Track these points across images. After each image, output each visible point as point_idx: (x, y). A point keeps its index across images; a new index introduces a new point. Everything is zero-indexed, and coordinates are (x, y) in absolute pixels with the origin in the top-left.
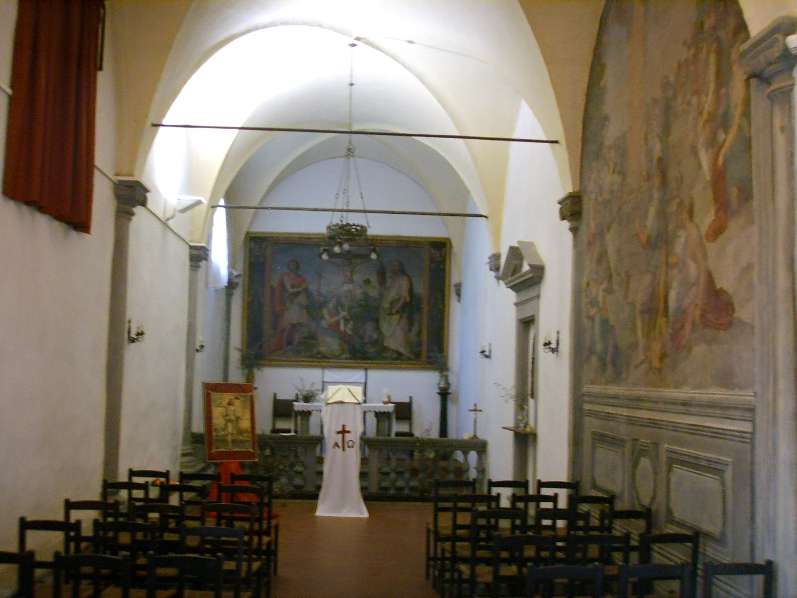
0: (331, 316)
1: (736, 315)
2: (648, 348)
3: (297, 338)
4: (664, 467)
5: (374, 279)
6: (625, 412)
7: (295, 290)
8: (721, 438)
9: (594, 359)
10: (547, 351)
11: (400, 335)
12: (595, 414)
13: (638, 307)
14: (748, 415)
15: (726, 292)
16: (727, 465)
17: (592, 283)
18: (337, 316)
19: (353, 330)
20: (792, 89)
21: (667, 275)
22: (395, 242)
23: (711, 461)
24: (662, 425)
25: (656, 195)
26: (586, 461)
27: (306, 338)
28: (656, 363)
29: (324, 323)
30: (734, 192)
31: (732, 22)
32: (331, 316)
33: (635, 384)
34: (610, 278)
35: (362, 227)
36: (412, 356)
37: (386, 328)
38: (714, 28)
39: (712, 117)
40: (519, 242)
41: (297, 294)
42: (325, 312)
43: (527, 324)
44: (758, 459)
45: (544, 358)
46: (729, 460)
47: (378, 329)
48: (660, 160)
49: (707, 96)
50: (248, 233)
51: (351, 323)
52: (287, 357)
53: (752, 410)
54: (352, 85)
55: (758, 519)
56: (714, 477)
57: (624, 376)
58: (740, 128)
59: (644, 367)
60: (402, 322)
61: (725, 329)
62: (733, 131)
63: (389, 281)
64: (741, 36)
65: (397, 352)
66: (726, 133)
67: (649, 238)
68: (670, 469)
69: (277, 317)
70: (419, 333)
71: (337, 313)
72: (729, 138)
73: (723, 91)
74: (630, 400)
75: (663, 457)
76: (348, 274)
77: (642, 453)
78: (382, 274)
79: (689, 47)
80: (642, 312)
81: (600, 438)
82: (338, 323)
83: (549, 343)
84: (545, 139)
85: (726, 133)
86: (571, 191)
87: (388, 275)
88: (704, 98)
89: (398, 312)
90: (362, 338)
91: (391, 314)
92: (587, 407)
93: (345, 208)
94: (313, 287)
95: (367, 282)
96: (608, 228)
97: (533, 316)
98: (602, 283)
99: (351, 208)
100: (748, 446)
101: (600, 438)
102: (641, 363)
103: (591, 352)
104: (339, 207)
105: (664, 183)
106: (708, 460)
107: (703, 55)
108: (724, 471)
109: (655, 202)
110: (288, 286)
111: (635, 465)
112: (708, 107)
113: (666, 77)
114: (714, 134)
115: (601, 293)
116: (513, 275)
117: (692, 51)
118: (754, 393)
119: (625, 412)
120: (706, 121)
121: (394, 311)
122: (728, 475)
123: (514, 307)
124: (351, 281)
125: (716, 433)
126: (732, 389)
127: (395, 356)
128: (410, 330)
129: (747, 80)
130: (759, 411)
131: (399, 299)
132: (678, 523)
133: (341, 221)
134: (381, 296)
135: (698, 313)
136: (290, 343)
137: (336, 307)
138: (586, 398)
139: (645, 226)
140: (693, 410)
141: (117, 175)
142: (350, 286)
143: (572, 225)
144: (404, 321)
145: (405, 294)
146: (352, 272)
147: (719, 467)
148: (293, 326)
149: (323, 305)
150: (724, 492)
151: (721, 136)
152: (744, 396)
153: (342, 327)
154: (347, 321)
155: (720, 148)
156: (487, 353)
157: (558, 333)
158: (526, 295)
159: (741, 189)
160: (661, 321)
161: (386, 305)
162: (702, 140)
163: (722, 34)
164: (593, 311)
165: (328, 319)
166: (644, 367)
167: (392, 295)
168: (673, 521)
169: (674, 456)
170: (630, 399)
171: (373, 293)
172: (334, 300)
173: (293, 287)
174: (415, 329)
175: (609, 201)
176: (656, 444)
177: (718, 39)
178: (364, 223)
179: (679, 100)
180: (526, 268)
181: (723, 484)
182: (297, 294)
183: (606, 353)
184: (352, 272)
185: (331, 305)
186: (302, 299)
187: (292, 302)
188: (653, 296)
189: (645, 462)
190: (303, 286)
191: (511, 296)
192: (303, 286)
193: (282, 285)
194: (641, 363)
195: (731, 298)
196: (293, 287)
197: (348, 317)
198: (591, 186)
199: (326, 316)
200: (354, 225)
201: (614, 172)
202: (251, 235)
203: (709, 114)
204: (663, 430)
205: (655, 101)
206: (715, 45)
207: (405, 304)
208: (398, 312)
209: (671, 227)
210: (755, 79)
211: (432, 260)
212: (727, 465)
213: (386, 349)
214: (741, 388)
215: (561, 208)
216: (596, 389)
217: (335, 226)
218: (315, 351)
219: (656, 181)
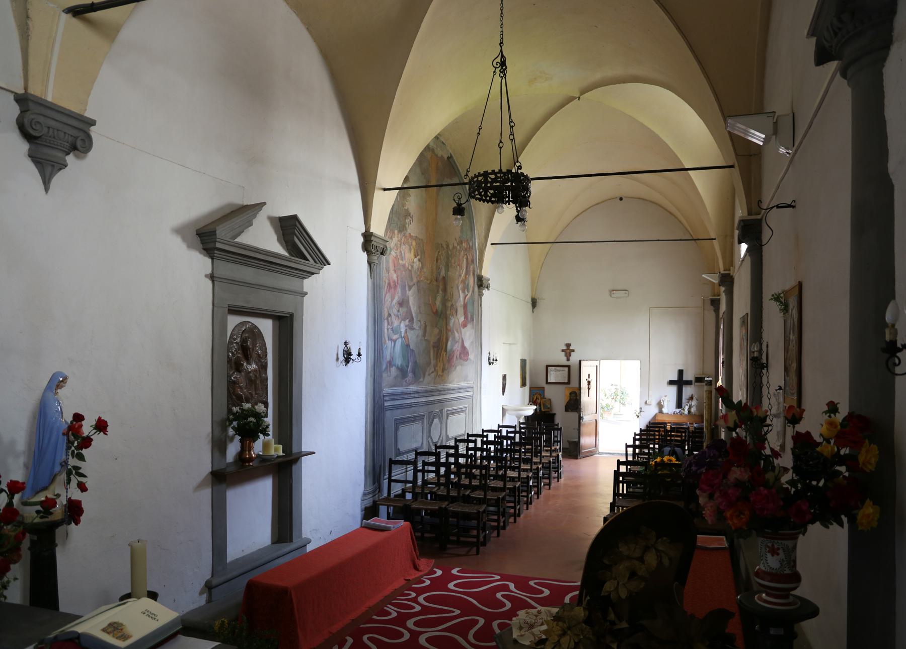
2: (436, 366)
6: (424, 399)
13: (432, 343)
28: (440, 373)
57: (421, 380)
59: (433, 375)
102: (432, 372)
119: (424, 399)
140: (456, 391)
152: (470, 384)
160: (443, 353)
169: (449, 412)
176: (441, 411)
188: (439, 340)
189: (436, 421)
194: (432, 372)
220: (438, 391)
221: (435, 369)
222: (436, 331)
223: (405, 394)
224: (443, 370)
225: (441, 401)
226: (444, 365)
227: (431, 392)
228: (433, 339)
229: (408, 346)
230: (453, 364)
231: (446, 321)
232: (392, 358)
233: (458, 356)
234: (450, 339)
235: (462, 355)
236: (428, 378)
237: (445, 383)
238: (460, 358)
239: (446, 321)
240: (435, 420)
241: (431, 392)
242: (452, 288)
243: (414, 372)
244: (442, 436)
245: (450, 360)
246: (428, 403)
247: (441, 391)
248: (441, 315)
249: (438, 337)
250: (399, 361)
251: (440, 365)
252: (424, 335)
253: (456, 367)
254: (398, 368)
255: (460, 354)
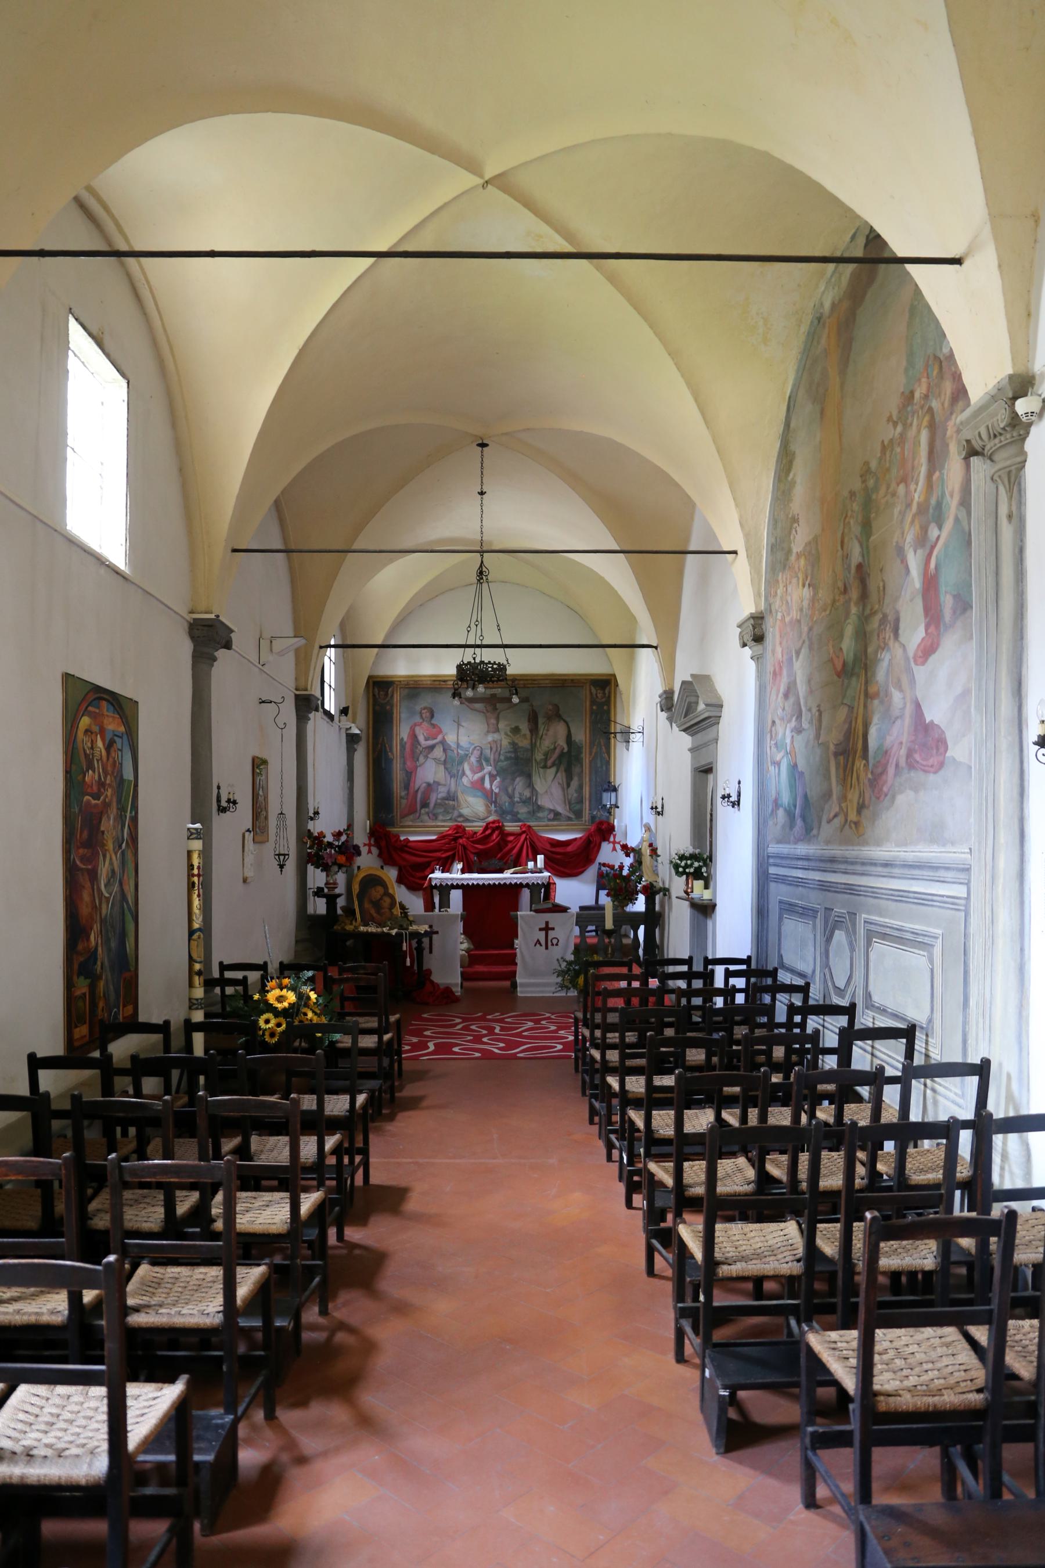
0: (475, 773)
1: (948, 754)
2: (843, 798)
3: (433, 799)
4: (862, 942)
5: (525, 728)
6: (817, 876)
7: (430, 743)
8: (932, 906)
9: (781, 812)
10: (726, 804)
11: (557, 792)
12: (782, 880)
13: (832, 747)
14: (962, 876)
15: (938, 726)
16: (937, 938)
17: (777, 721)
18: (480, 771)
19: (498, 787)
20: (1024, 466)
21: (865, 706)
22: (547, 682)
23: (917, 934)
24: (861, 891)
25: (854, 610)
26: (772, 937)
27: (444, 799)
28: (853, 816)
29: (465, 780)
30: (947, 602)
31: (948, 387)
32: (475, 773)
33: (828, 842)
34: (799, 716)
35: (499, 665)
36: (573, 816)
37: (539, 785)
38: (926, 397)
39: (923, 509)
40: (692, 676)
41: (432, 748)
42: (466, 767)
43: (704, 771)
44: (972, 929)
45: (723, 811)
46: (940, 932)
47: (530, 785)
48: (860, 566)
49: (917, 484)
50: (370, 677)
51: (498, 779)
52: (422, 821)
53: (967, 870)
54: (482, 493)
55: (972, 1002)
56: (921, 953)
57: (815, 832)
58: (957, 520)
59: (837, 822)
60: (559, 774)
61: (936, 772)
62: (949, 524)
63: (541, 727)
64: (961, 404)
65: (551, 811)
66: (940, 528)
67: (844, 664)
68: (869, 943)
69: (410, 775)
70: (581, 787)
71: (481, 768)
72: (942, 535)
73: (937, 474)
74: (822, 861)
75: (861, 932)
76: (493, 721)
77: (837, 925)
78: (533, 719)
79: (895, 424)
80: (836, 754)
81: (789, 908)
82: (483, 779)
83: (729, 796)
84: (617, 548)
85: (940, 528)
86: (754, 611)
87: (541, 720)
88: (912, 487)
89: (553, 765)
90: (511, 797)
91: (545, 767)
92: (772, 870)
93: (479, 642)
94: (451, 739)
95: (516, 730)
96: (798, 653)
97: (711, 763)
98: (790, 721)
99: (485, 643)
100: (963, 914)
101: (789, 908)
102: (836, 816)
103: (777, 804)
104: (471, 642)
105: (864, 596)
106: (913, 933)
107: (912, 433)
108: (932, 946)
109: (853, 619)
110: (421, 738)
111: (829, 939)
112: (917, 497)
113: (867, 463)
114: (924, 530)
115: (788, 733)
116: (686, 716)
117: (899, 429)
118: (970, 849)
119: (817, 876)
120: (914, 516)
121: (549, 763)
122: (937, 951)
123: (689, 754)
124: (497, 730)
125: (923, 899)
126: (944, 845)
127: (552, 816)
128: (568, 785)
129: (967, 458)
130: (974, 871)
131: (555, 748)
132: (878, 1008)
133: (474, 659)
134: (533, 746)
135: (903, 752)
136: (425, 804)
137: (479, 761)
138: (771, 861)
139: (841, 649)
140: (897, 871)
141: (192, 612)
142: (496, 736)
143: (753, 652)
144: (561, 776)
145: (562, 742)
146: (498, 719)
147: (926, 940)
148: (429, 785)
149: (463, 759)
150: (932, 970)
151: (933, 532)
153: (487, 785)
154: (492, 778)
155: (933, 547)
156: (659, 810)
157: (739, 783)
158: (702, 737)
159: (957, 597)
160: (859, 764)
161: (539, 756)
162: (910, 538)
163: (935, 404)
164: (778, 758)
165: (470, 776)
166: (837, 822)
167: (546, 744)
168: (873, 1006)
169: (873, 928)
170: (821, 860)
171: (524, 743)
172: (477, 753)
173: (426, 739)
174: (575, 783)
175: (799, 621)
176: (853, 915)
177: (930, 410)
178: (503, 661)
179: (882, 491)
180: (701, 706)
181: (931, 961)
182: (432, 748)
183: (795, 806)
184: (498, 719)
185: (473, 759)
186: (438, 752)
187: (426, 757)
188: (849, 734)
189: (839, 936)
190: (440, 738)
191: (686, 740)
192: (440, 738)
193: (414, 736)
194: (836, 816)
195: (943, 732)
196: (426, 739)
197: (495, 773)
198: (777, 604)
199: (468, 772)
200: (489, 663)
201: (804, 586)
202: (375, 680)
203: (919, 504)
204: (862, 897)
205: (852, 494)
206: (927, 418)
207: (562, 755)
208: (553, 765)
209: (870, 650)
210: (976, 457)
211: (593, 702)
212: (937, 938)
213: (540, 808)
214: (953, 844)
215: (740, 633)
216: (784, 849)
217: (466, 665)
218: (456, 814)
219: (854, 594)
220: (846, 862)
221: (841, 808)
222: (842, 713)
223: (782, 858)
224: (861, 808)
225: (851, 890)
226: (861, 795)
227: (830, 863)
228: (833, 737)
229: (795, 766)
230: (885, 789)
231: (866, 674)
232: (778, 793)
233: (903, 762)
234: (875, 720)
235: (917, 757)
236: (827, 830)
237: (865, 843)
238: (911, 766)
239: (866, 674)
240: (837, 932)
241: (830, 863)
242: (881, 570)
243: (804, 818)
244: (852, 983)
245: (876, 780)
246: (825, 887)
247: (853, 863)
248: (853, 669)
249: (846, 726)
250: (786, 798)
251: (853, 796)
252: (818, 736)
253: (894, 798)
254: (785, 810)
255: (910, 754)
